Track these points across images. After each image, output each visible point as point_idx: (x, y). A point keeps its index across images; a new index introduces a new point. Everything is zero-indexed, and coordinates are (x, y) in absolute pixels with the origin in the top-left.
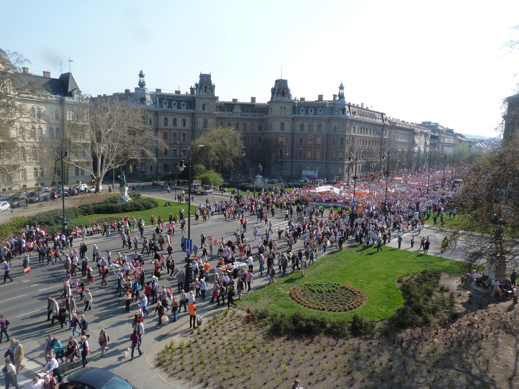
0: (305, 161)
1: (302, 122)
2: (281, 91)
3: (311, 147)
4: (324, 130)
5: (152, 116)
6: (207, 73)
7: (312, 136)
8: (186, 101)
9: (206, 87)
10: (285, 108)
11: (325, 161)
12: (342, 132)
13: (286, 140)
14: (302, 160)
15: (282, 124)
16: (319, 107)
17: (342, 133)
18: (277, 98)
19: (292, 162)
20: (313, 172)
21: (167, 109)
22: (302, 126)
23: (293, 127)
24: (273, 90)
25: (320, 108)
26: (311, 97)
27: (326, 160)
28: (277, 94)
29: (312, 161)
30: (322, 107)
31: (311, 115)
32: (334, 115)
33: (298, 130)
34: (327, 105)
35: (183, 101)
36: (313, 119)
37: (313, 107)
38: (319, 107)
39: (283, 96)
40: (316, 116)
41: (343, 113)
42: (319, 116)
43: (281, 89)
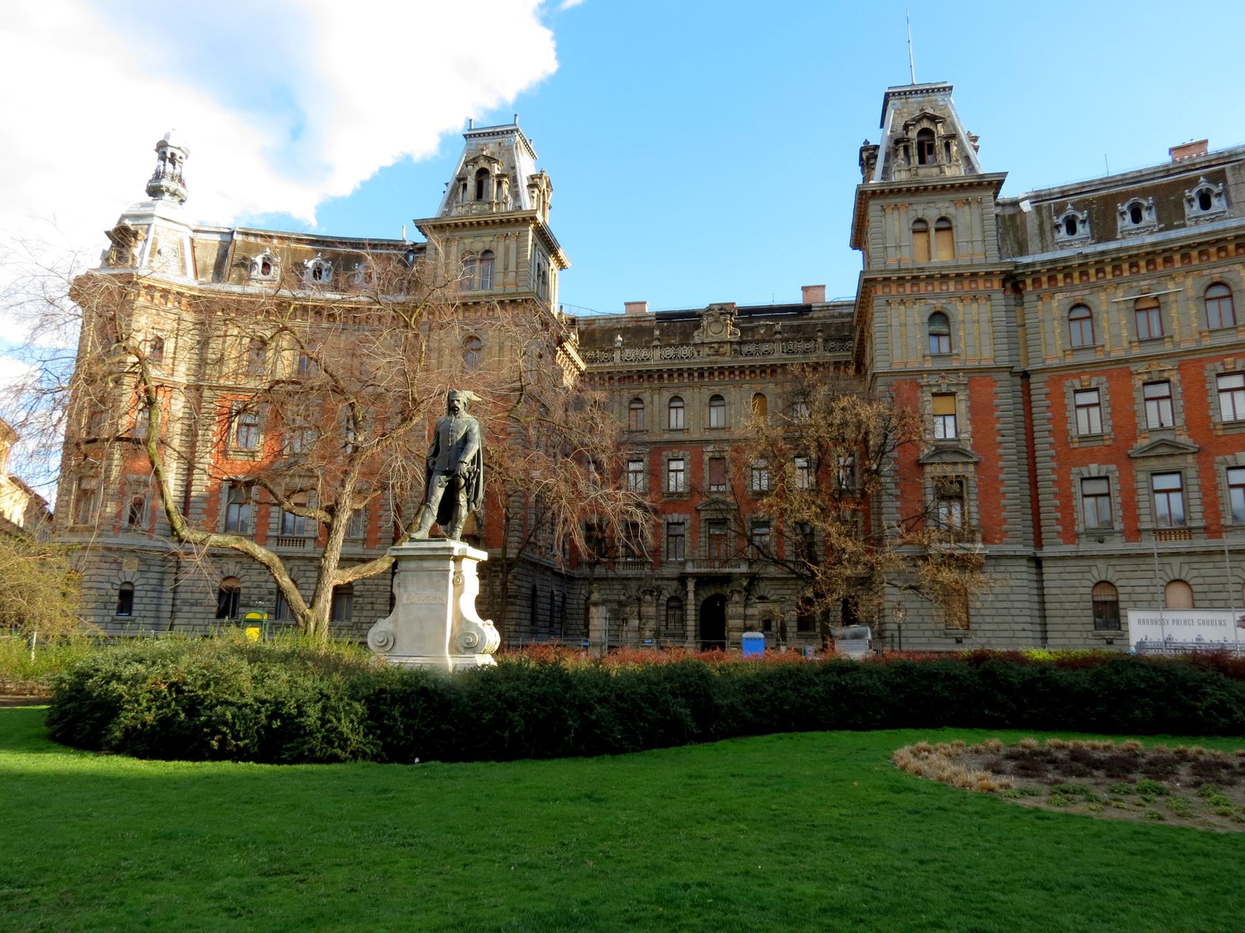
0: (1133, 547)
2: (913, 134)
3: (1177, 449)
10: (945, 225)
13: (979, 413)
15: (939, 316)
19: (1038, 562)
23: (1018, 333)
29: (1200, 543)
37: (1144, 193)
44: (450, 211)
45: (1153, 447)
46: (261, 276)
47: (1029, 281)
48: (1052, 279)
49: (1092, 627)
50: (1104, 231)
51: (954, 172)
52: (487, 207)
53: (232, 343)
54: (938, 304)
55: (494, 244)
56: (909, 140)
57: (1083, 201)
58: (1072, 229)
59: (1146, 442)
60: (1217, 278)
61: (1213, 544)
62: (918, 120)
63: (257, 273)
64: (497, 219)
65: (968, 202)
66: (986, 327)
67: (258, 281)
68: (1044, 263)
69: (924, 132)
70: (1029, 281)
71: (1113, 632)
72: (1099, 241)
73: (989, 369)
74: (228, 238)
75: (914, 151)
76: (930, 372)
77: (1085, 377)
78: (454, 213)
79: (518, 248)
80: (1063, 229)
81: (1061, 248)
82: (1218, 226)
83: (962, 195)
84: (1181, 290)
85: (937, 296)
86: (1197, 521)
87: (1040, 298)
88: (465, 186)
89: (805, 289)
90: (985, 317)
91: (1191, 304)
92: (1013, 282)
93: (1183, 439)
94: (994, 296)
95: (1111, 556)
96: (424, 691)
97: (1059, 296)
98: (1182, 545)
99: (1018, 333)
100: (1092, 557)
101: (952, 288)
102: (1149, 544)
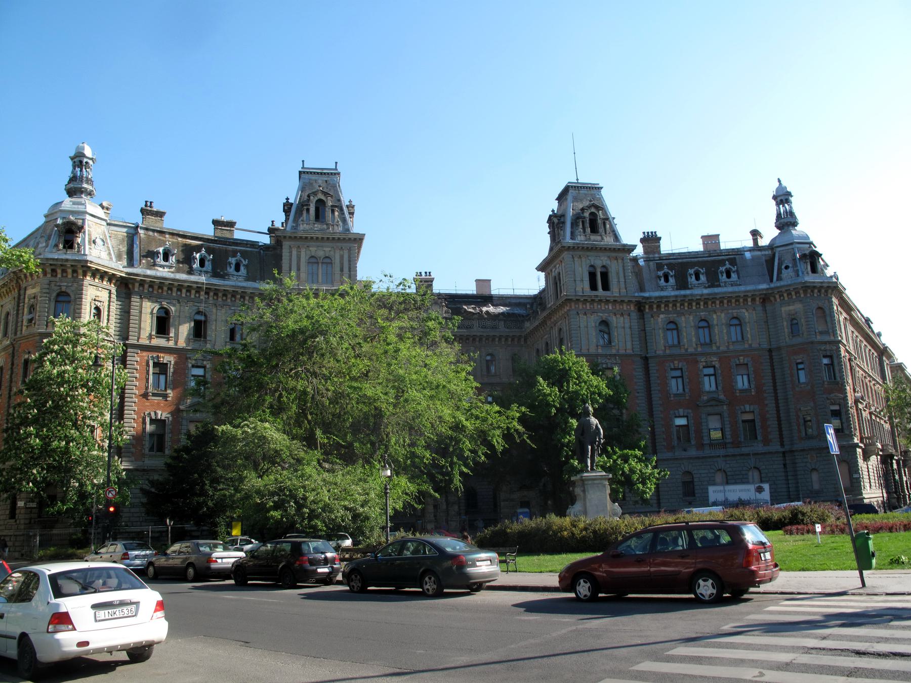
0: (700, 453)
1: (673, 316)
2: (587, 214)
3: (719, 402)
4: (754, 337)
5: (104, 296)
6: (326, 164)
7: (715, 360)
8: (244, 254)
9: (320, 202)
11: (776, 447)
12: (821, 333)
14: (693, 452)
15: (605, 323)
16: (722, 263)
17: (826, 338)
18: (573, 236)
20: (752, 487)
21: (171, 276)
22: (673, 325)
23: (644, 336)
24: (555, 223)
25: (728, 266)
26: (680, 241)
27: (782, 445)
28: (574, 224)
29: (731, 451)
30: (733, 262)
31: (699, 289)
32: (779, 278)
33: (661, 342)
34: (748, 255)
35: (234, 254)
36: (706, 300)
37: (702, 264)
38: (722, 263)
39: (594, 229)
40: (716, 290)
41: (814, 269)
42: (730, 289)
43: (580, 218)
44: (297, 226)
45: (708, 401)
46: (163, 263)
47: (647, 307)
48: (659, 307)
49: (681, 496)
50: (682, 284)
51: (609, 240)
52: (325, 226)
53: (146, 312)
54: (604, 316)
55: (332, 253)
56: (585, 218)
57: (670, 264)
58: (667, 280)
59: (705, 398)
60: (735, 315)
61: (737, 451)
62: (589, 207)
63: (160, 260)
64: (336, 237)
65: (616, 259)
66: (628, 331)
67: (161, 266)
68: (656, 298)
69: (592, 214)
70: (647, 307)
71: (692, 498)
72: (680, 289)
73: (630, 355)
74: (132, 231)
75: (588, 225)
76: (601, 355)
77: (676, 362)
78: (301, 227)
79: (349, 257)
80: (663, 279)
81: (662, 290)
82: (736, 289)
83: (614, 254)
84: (719, 318)
85: (603, 312)
86: (729, 439)
87: (652, 316)
88: (308, 210)
89: (478, 281)
90: (627, 325)
91: (724, 327)
92: (640, 306)
93: (722, 397)
94: (632, 314)
95: (691, 458)
96: (237, 566)
97: (662, 316)
98: (722, 452)
99: (644, 336)
100: (682, 459)
101: (610, 308)
102: (707, 452)
